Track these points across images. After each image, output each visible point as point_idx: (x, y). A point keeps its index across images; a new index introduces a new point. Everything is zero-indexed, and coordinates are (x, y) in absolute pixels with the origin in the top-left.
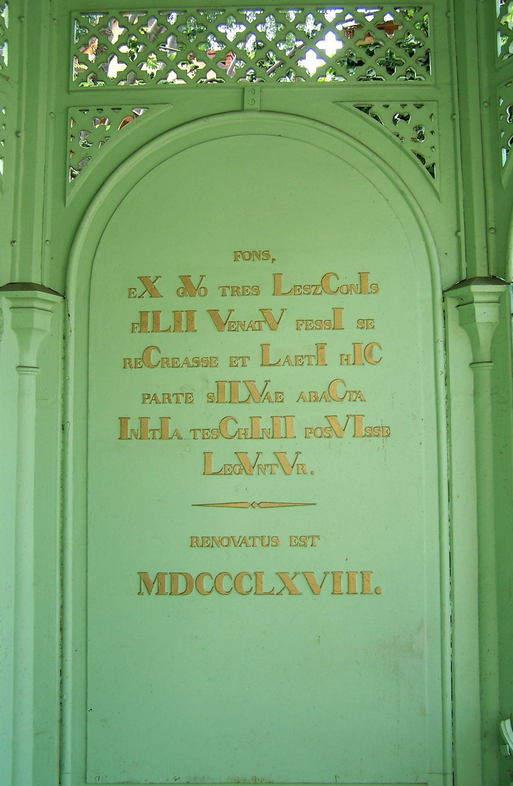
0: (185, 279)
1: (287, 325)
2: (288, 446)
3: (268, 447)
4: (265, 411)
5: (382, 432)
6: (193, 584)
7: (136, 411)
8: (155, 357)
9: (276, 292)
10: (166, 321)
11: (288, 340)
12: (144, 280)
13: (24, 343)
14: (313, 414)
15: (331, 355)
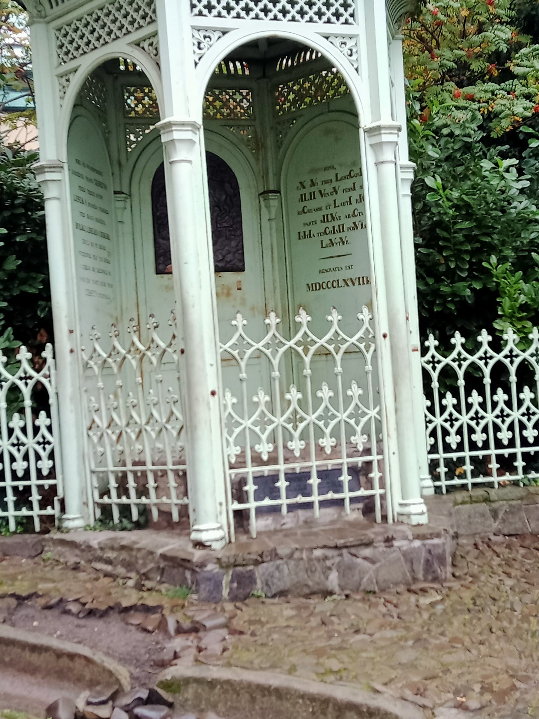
0: (312, 180)
1: (340, 192)
2: (341, 235)
3: (338, 235)
4: (336, 223)
8: (306, 210)
9: (337, 180)
11: (341, 197)
12: (301, 183)
13: (269, 212)
14: (349, 223)
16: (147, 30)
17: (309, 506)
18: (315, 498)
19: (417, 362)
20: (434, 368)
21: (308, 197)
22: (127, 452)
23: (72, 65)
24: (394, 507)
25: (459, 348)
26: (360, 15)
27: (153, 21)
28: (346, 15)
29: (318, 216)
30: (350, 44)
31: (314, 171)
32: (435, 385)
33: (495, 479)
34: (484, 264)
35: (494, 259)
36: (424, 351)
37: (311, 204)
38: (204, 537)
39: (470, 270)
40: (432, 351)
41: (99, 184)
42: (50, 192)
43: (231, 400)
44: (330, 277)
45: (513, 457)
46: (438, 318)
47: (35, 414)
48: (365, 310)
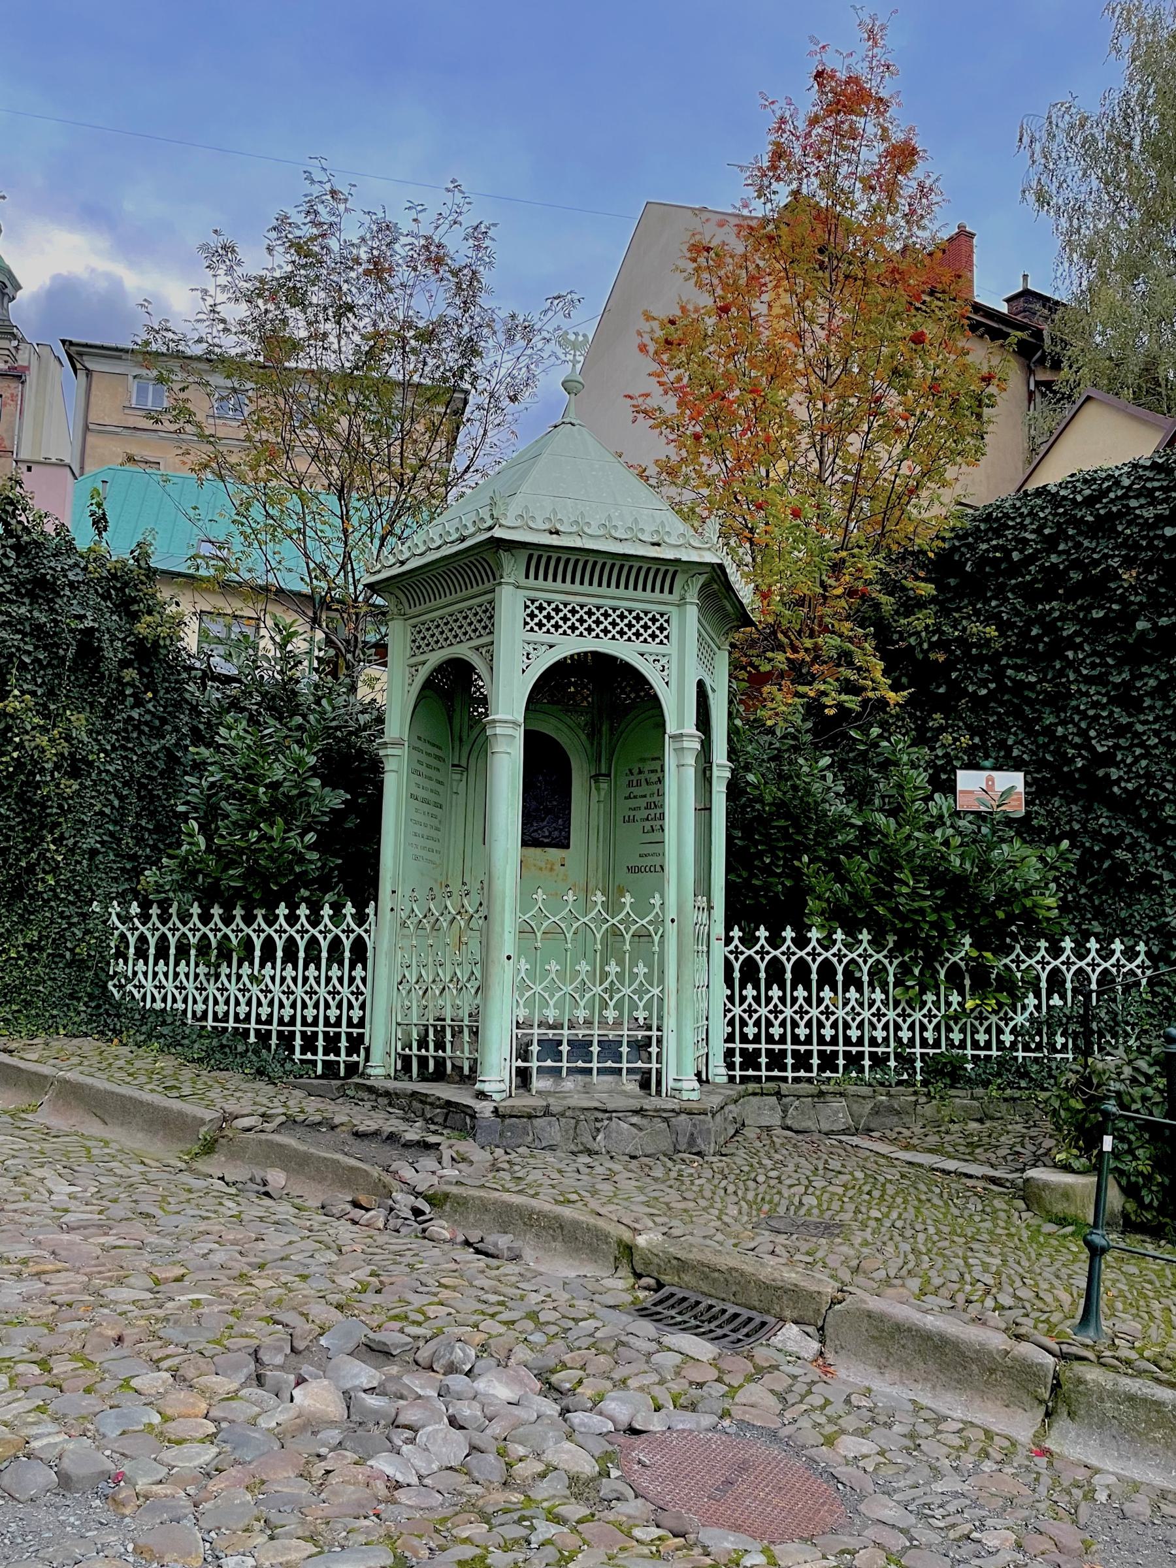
16: (485, 640)
17: (589, 1071)
18: (595, 1065)
19: (719, 951)
20: (737, 959)
22: (431, 1006)
23: (422, 658)
24: (668, 1082)
25: (762, 941)
26: (673, 637)
27: (491, 633)
28: (661, 637)
30: (663, 661)
31: (643, 760)
32: (737, 975)
33: (789, 1074)
34: (796, 863)
35: (805, 859)
36: (728, 940)
37: (637, 791)
38: (486, 1087)
39: (784, 866)
40: (736, 942)
41: (438, 757)
42: (390, 765)
43: (524, 965)
45: (809, 1053)
46: (743, 909)
47: (352, 967)
48: (657, 896)
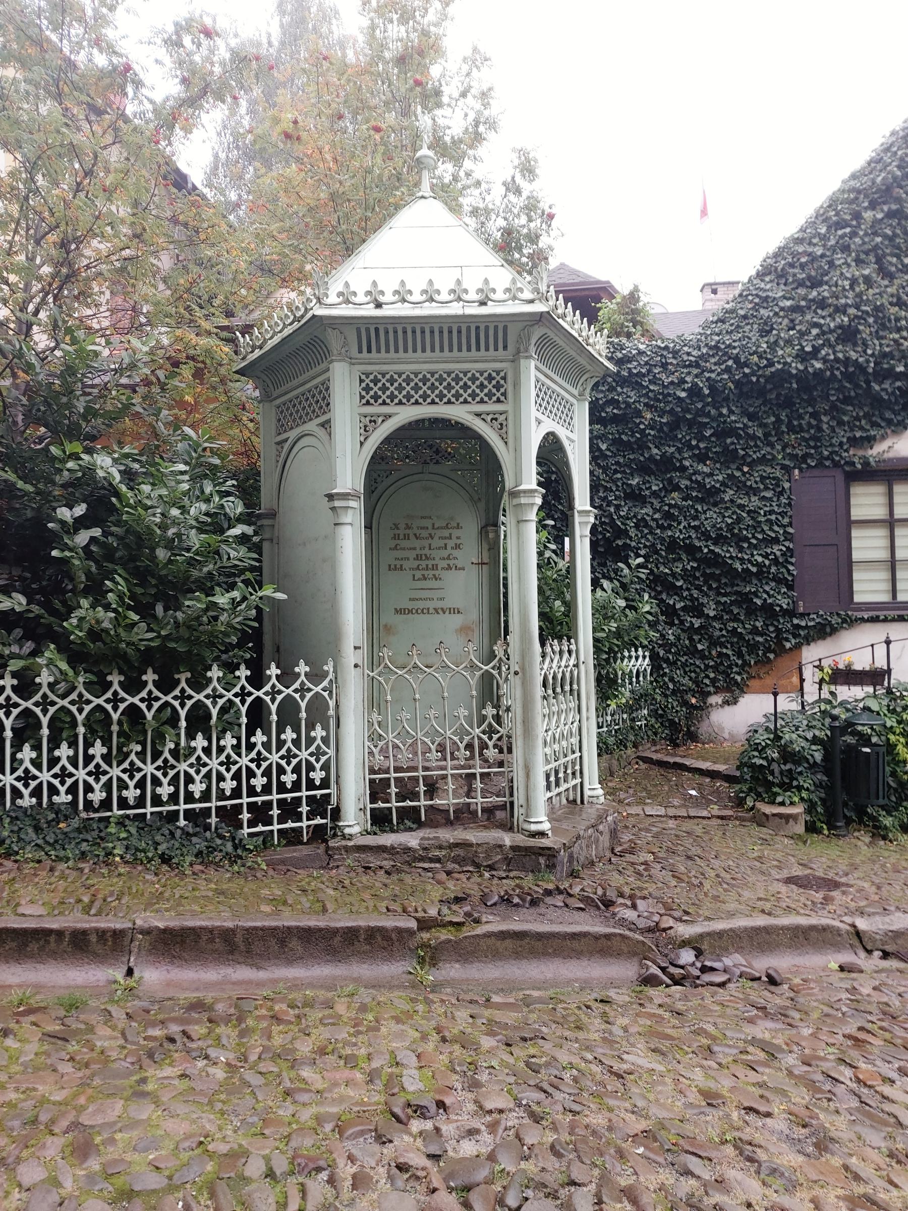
1: (436, 538)
3: (431, 573)
4: (430, 563)
5: (463, 569)
6: (410, 611)
7: (393, 563)
10: (401, 537)
11: (436, 543)
14: (444, 564)
15: (449, 547)
21: (401, 537)
29: (412, 554)
44: (421, 605)
